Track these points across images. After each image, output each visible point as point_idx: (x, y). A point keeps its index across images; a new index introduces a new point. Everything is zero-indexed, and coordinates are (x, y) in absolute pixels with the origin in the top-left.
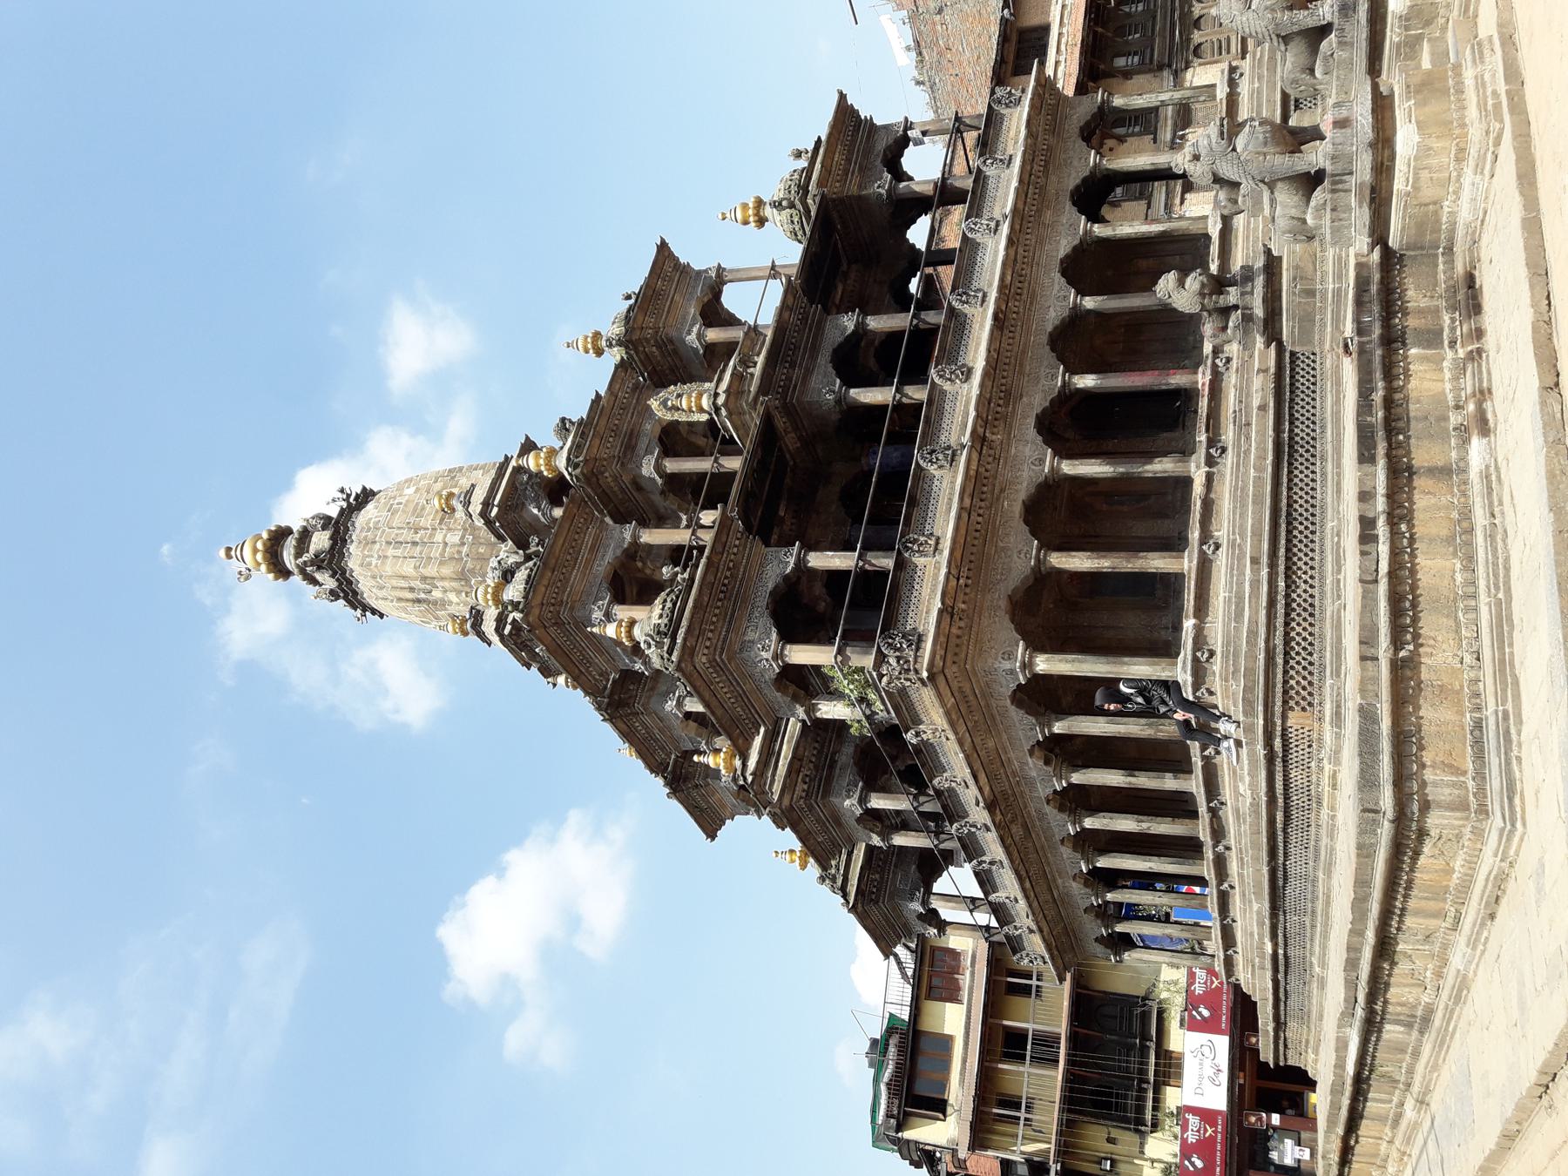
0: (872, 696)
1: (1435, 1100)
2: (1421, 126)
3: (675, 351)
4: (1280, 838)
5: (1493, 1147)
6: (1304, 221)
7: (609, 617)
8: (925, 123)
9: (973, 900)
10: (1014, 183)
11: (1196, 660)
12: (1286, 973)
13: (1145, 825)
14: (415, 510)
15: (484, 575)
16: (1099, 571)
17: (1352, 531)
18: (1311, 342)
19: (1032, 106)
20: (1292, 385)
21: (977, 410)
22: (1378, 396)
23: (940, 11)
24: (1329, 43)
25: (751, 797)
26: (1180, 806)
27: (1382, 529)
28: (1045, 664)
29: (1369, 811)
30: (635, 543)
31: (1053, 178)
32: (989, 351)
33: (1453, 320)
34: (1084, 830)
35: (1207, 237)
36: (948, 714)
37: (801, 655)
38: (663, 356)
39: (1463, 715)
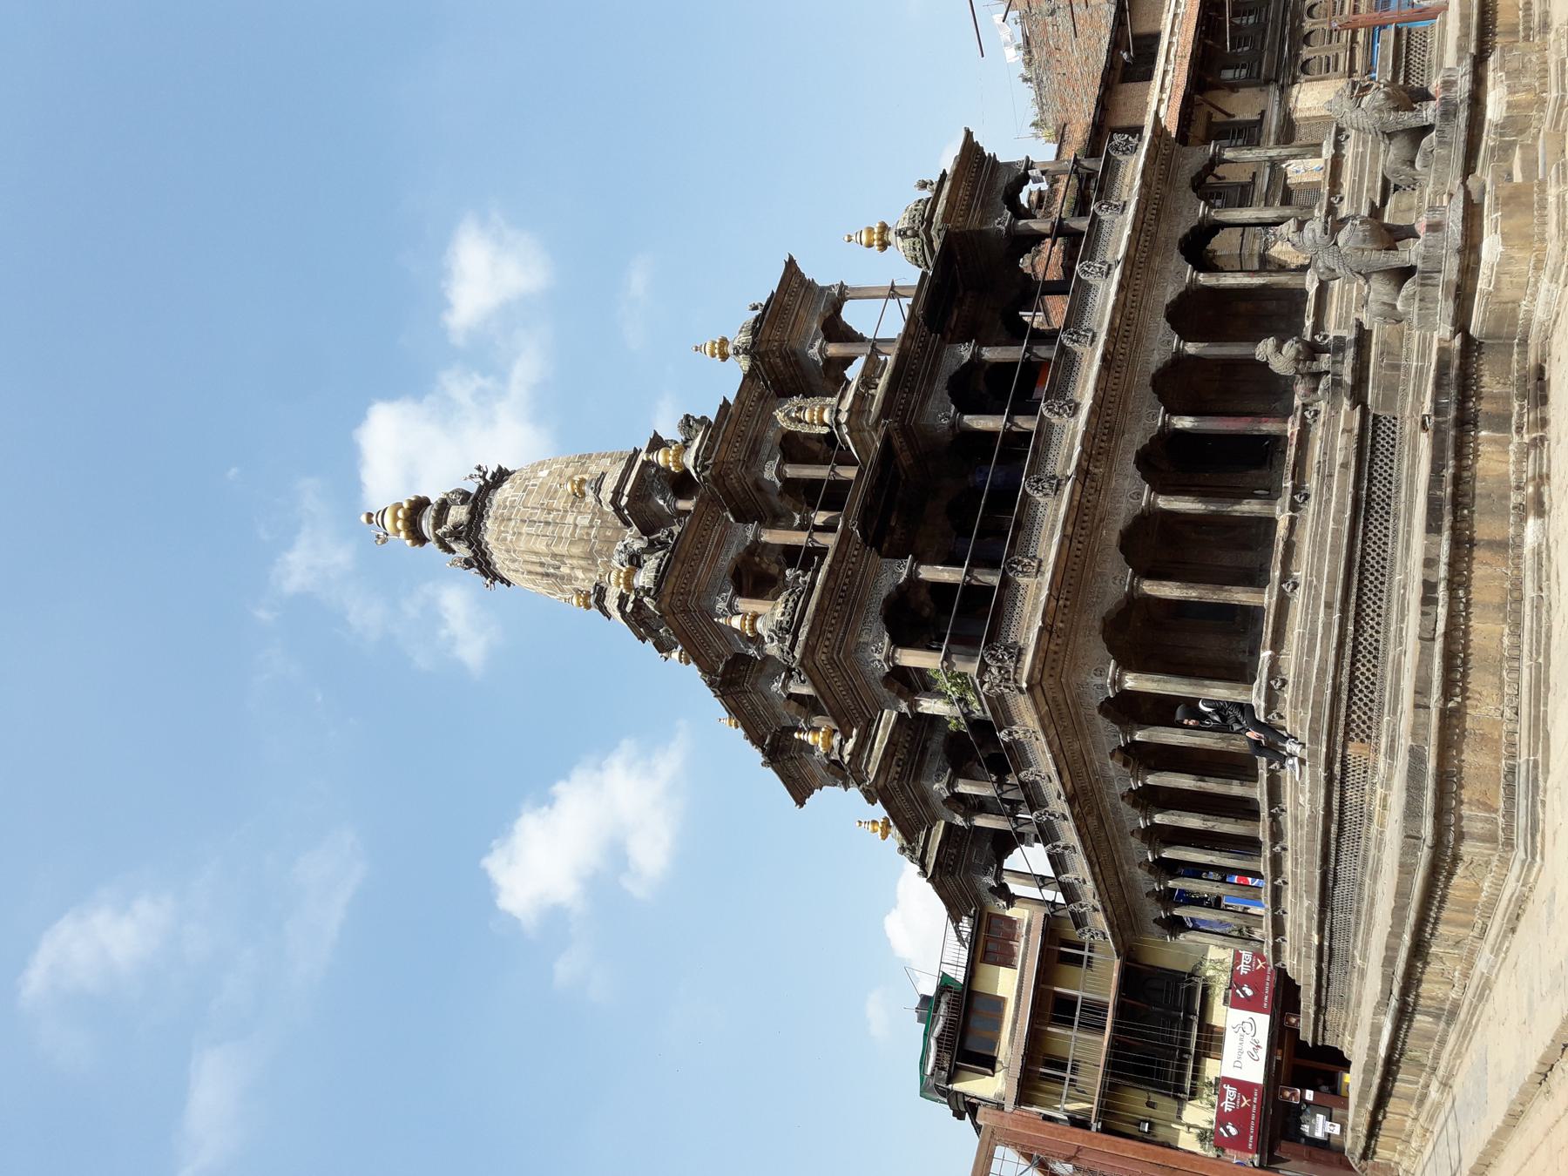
0: (970, 697)
2: (1505, 238)
3: (797, 362)
4: (1333, 847)
6: (1394, 307)
8: (1045, 163)
9: (1043, 878)
10: (1127, 231)
11: (1269, 688)
12: (1330, 963)
13: (1210, 824)
15: (610, 556)
16: (1184, 600)
17: (1415, 595)
19: (1148, 156)
20: (1373, 445)
21: (1082, 445)
22: (1448, 473)
23: (1053, 13)
25: (841, 773)
26: (1245, 809)
27: (1442, 593)
28: (1131, 682)
29: (1411, 837)
31: (1164, 226)
32: (1096, 390)
33: (1522, 407)
35: (1304, 293)
36: (1041, 720)
37: (911, 658)
39: (1498, 760)
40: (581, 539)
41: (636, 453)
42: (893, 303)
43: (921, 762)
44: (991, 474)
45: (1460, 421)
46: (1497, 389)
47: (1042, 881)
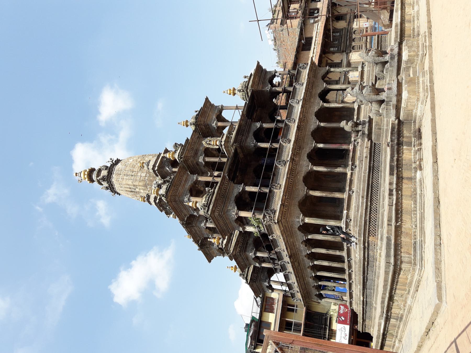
0: (261, 226)
1: (403, 340)
4: (366, 269)
5: (416, 349)
6: (379, 111)
7: (189, 200)
8: (280, 72)
9: (282, 283)
10: (304, 91)
11: (346, 222)
13: (330, 264)
14: (133, 166)
15: (152, 186)
16: (321, 197)
18: (380, 141)
20: (374, 151)
22: (395, 158)
23: (282, 31)
24: (387, 65)
25: (222, 251)
26: (340, 259)
28: (307, 220)
29: (388, 263)
30: (197, 180)
31: (314, 90)
33: (415, 140)
34: (314, 264)
36: (281, 232)
37: (243, 214)
38: (205, 128)
40: (142, 180)
41: (160, 154)
42: (237, 111)
43: (246, 247)
44: (266, 160)
45: (398, 144)
46: (408, 135)
47: (282, 284)
